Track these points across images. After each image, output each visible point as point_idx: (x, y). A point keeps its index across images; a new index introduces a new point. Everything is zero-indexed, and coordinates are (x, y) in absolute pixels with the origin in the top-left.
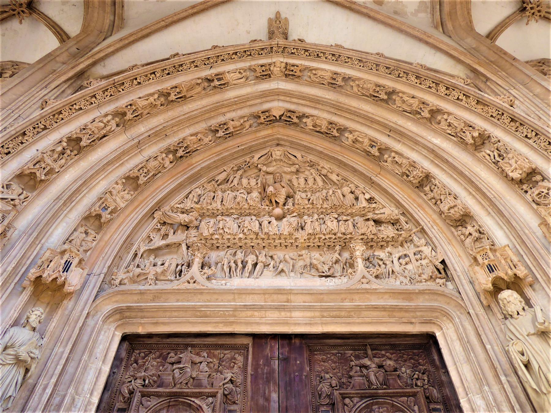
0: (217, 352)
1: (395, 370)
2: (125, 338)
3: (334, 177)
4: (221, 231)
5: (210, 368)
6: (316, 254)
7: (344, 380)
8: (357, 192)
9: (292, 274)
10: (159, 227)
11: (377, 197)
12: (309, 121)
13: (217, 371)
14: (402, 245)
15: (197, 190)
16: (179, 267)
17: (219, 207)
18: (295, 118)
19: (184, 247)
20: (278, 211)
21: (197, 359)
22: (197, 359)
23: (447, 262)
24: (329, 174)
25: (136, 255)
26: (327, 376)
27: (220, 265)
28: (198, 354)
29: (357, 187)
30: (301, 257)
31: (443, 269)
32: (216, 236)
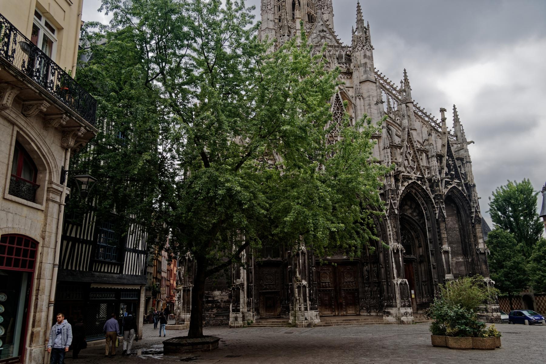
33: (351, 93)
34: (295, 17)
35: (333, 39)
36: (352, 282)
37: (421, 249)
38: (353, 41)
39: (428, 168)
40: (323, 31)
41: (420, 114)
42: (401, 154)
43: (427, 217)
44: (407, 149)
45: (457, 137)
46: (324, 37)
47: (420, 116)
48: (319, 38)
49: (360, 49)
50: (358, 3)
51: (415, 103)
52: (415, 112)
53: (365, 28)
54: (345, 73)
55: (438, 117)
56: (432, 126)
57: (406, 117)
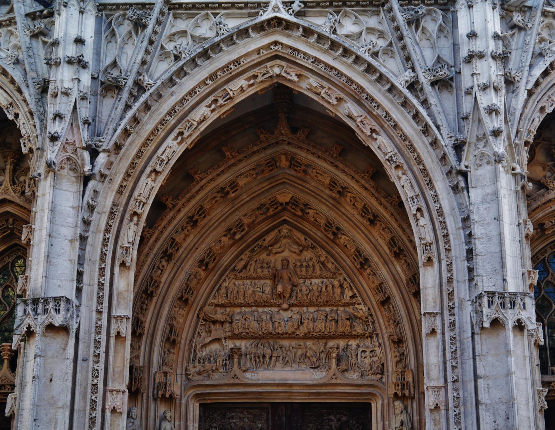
0: (252, 411)
1: (347, 422)
2: (201, 405)
3: (330, 265)
4: (247, 331)
5: (249, 420)
6: (309, 343)
7: (319, 427)
8: (345, 286)
9: (294, 365)
10: (203, 323)
11: (358, 295)
12: (311, 211)
13: (253, 422)
14: (367, 337)
15: (225, 284)
16: (225, 362)
17: (242, 302)
18: (298, 210)
19: (223, 340)
20: (285, 306)
21: (242, 416)
22: (242, 416)
23: (385, 365)
24: (325, 262)
25: (195, 351)
26: (311, 425)
27: (248, 356)
28: (242, 413)
29: (345, 279)
30: (300, 347)
31: (382, 370)
32: (244, 334)
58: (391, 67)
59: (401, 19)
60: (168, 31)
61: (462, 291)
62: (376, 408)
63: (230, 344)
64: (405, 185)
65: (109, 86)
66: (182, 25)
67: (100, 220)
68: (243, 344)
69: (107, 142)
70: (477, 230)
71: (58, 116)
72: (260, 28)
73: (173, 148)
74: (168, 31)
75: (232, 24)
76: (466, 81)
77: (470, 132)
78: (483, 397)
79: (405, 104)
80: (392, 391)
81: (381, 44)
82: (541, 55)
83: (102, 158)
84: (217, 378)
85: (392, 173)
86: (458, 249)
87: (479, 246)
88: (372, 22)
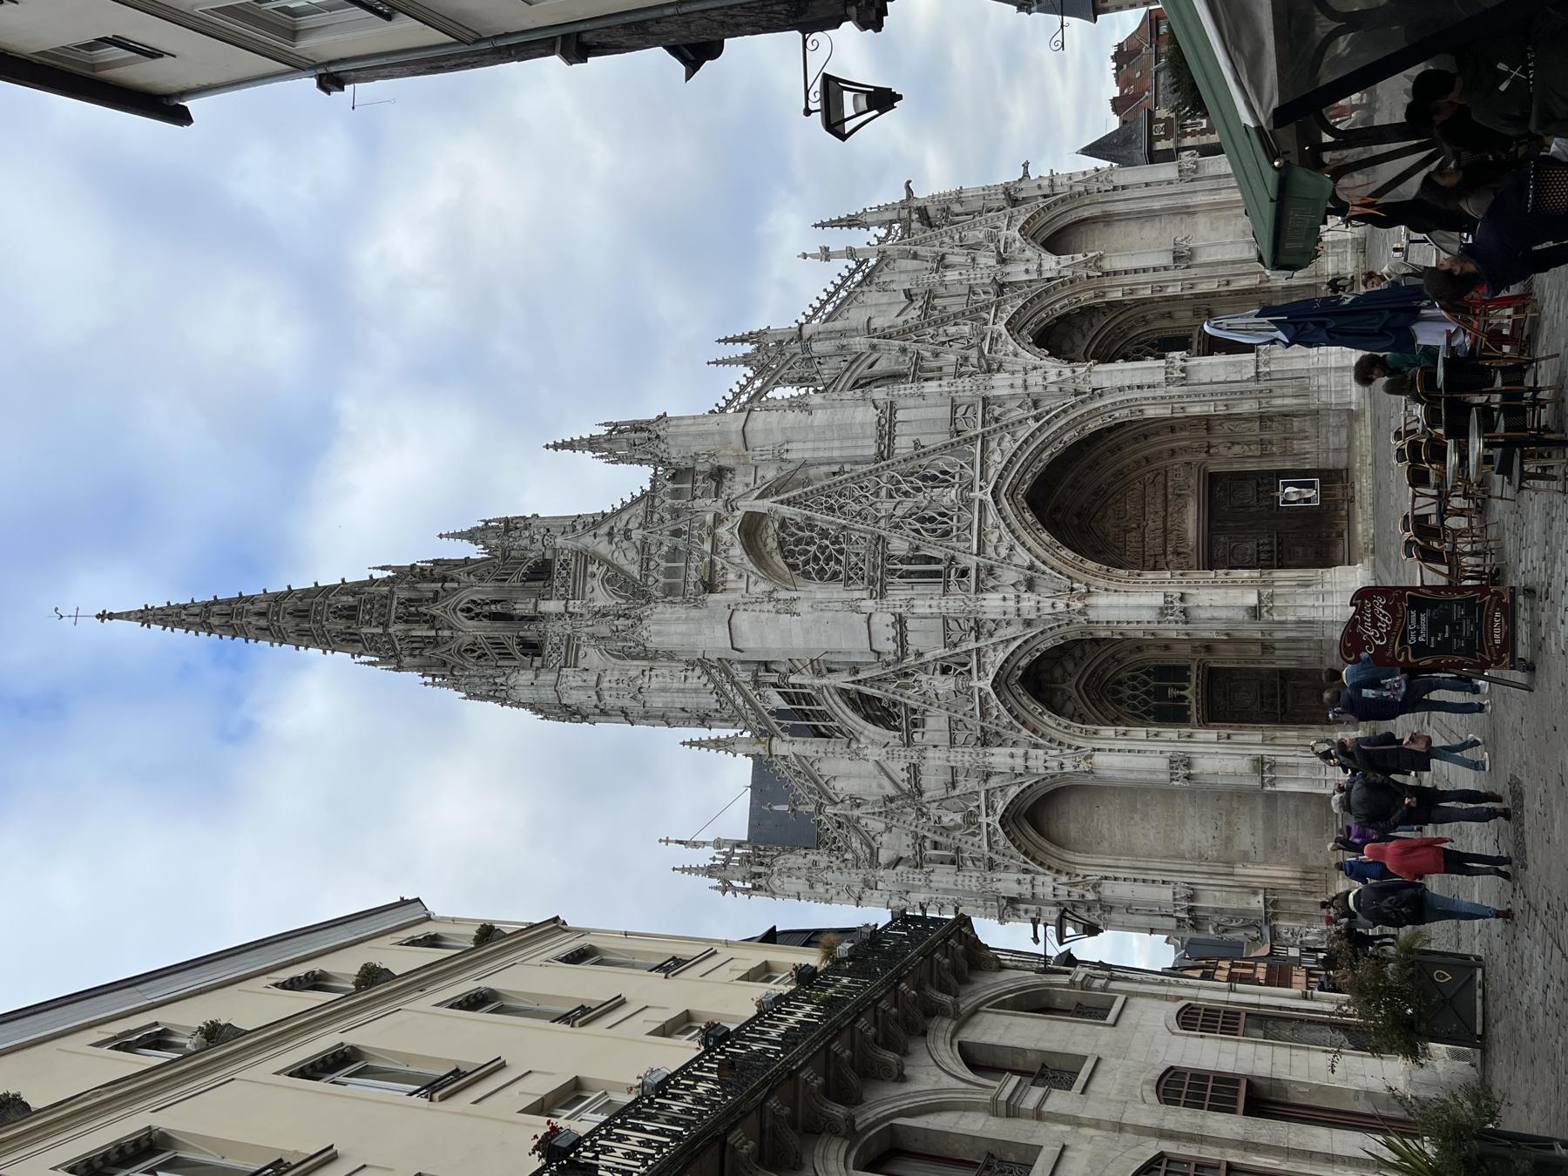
31: (1189, 463)
33: (770, 474)
34: (532, 613)
35: (632, 511)
36: (1258, 485)
37: (1178, 315)
38: (640, 462)
39: (971, 290)
40: (610, 534)
41: (829, 308)
42: (936, 355)
43: (1096, 297)
44: (923, 341)
45: (892, 222)
46: (627, 535)
47: (836, 309)
48: (625, 544)
49: (663, 446)
50: (547, 447)
51: (802, 320)
52: (826, 321)
53: (610, 432)
54: (719, 484)
55: (841, 266)
56: (864, 278)
57: (844, 342)
58: (1023, 433)
59: (994, 426)
60: (994, 555)
61: (1159, 392)
62: (1212, 469)
63: (1170, 557)
64: (1093, 426)
65: (1030, 585)
66: (990, 551)
67: (1113, 585)
68: (1170, 549)
69: (1068, 582)
70: (1127, 383)
71: (1053, 606)
72: (996, 503)
73: (1066, 553)
74: (994, 555)
75: (992, 517)
76: (1040, 389)
77: (1070, 387)
78: (1222, 378)
79: (1048, 422)
80: (1204, 455)
81: (1008, 437)
82: (1016, 355)
83: (1076, 585)
84: (1193, 561)
85: (1087, 432)
86: (1137, 394)
87: (1137, 382)
88: (993, 445)
